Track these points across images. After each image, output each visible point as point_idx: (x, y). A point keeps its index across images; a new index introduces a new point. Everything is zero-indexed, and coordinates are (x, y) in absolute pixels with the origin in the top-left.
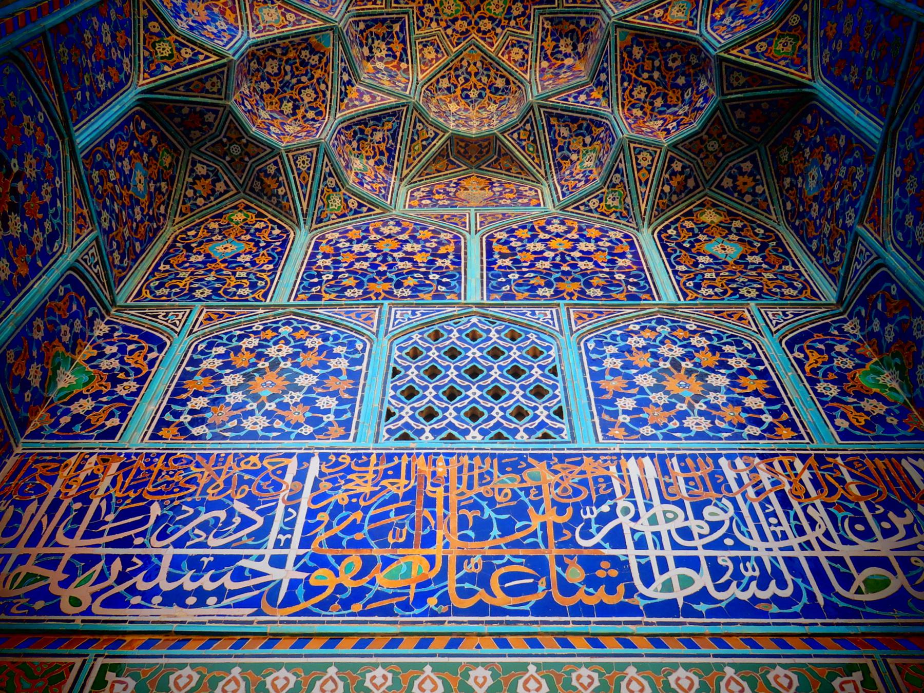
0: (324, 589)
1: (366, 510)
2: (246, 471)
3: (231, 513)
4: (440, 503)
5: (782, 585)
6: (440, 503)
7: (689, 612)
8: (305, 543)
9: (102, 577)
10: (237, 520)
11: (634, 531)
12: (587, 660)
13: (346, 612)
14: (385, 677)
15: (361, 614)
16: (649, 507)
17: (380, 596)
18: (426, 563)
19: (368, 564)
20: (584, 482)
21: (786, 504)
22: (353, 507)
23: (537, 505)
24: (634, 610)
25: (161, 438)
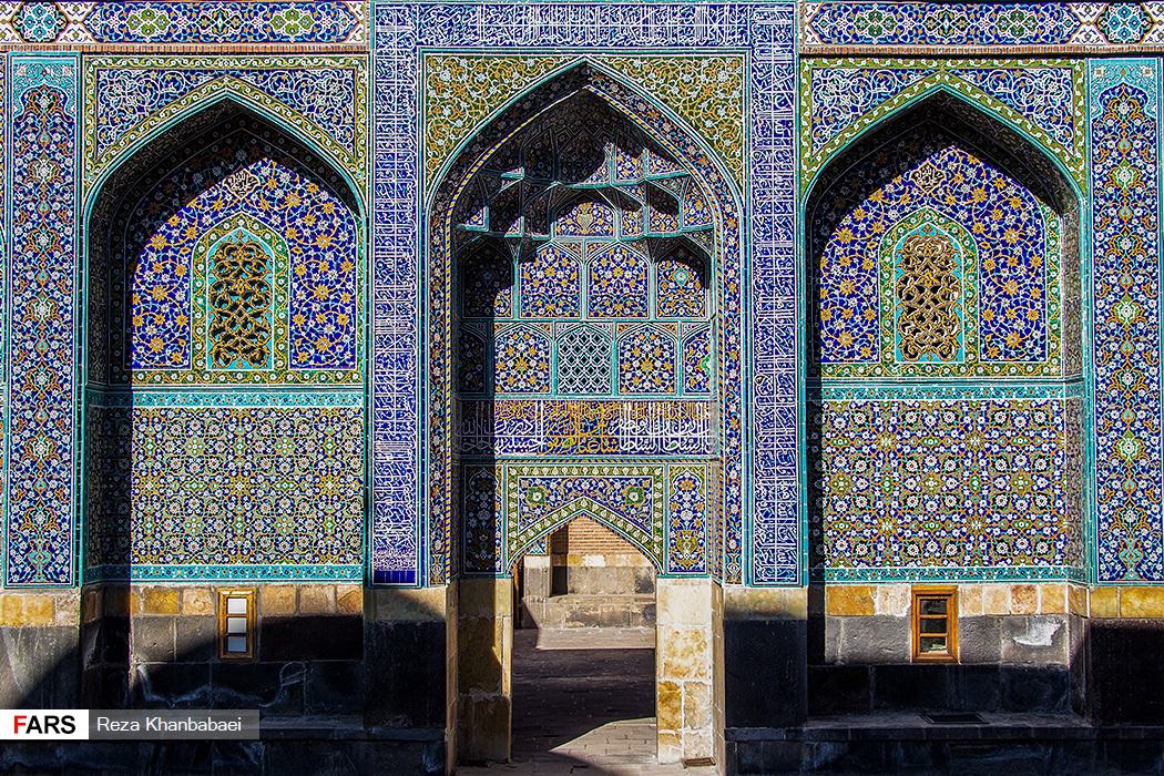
19: (560, 439)
21: (661, 420)
22: (554, 421)
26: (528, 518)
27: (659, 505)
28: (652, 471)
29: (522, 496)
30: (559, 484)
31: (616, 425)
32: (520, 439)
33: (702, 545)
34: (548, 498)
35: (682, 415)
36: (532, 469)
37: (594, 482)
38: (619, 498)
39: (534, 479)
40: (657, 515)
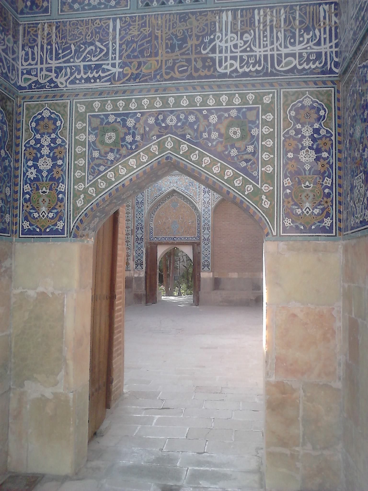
0: (128, 74)
1: (137, 42)
2: (97, 27)
3: (96, 47)
4: (160, 37)
5: (259, 66)
6: (160, 37)
7: (230, 76)
8: (120, 58)
9: (66, 75)
10: (98, 50)
11: (219, 46)
12: (200, 93)
13: (135, 82)
14: (147, 101)
15: (139, 82)
16: (226, 35)
17: (144, 76)
18: (156, 63)
19: (140, 64)
20: (206, 25)
22: (133, 41)
23: (190, 36)
24: (214, 77)
25: (64, 11)
26: (99, 165)
27: (269, 143)
28: (258, 99)
29: (92, 138)
30: (138, 120)
31: (213, 40)
32: (90, 66)
33: (329, 195)
34: (123, 139)
35: (301, 22)
36: (104, 104)
37: (182, 116)
38: (214, 135)
39: (107, 116)
40: (265, 156)
